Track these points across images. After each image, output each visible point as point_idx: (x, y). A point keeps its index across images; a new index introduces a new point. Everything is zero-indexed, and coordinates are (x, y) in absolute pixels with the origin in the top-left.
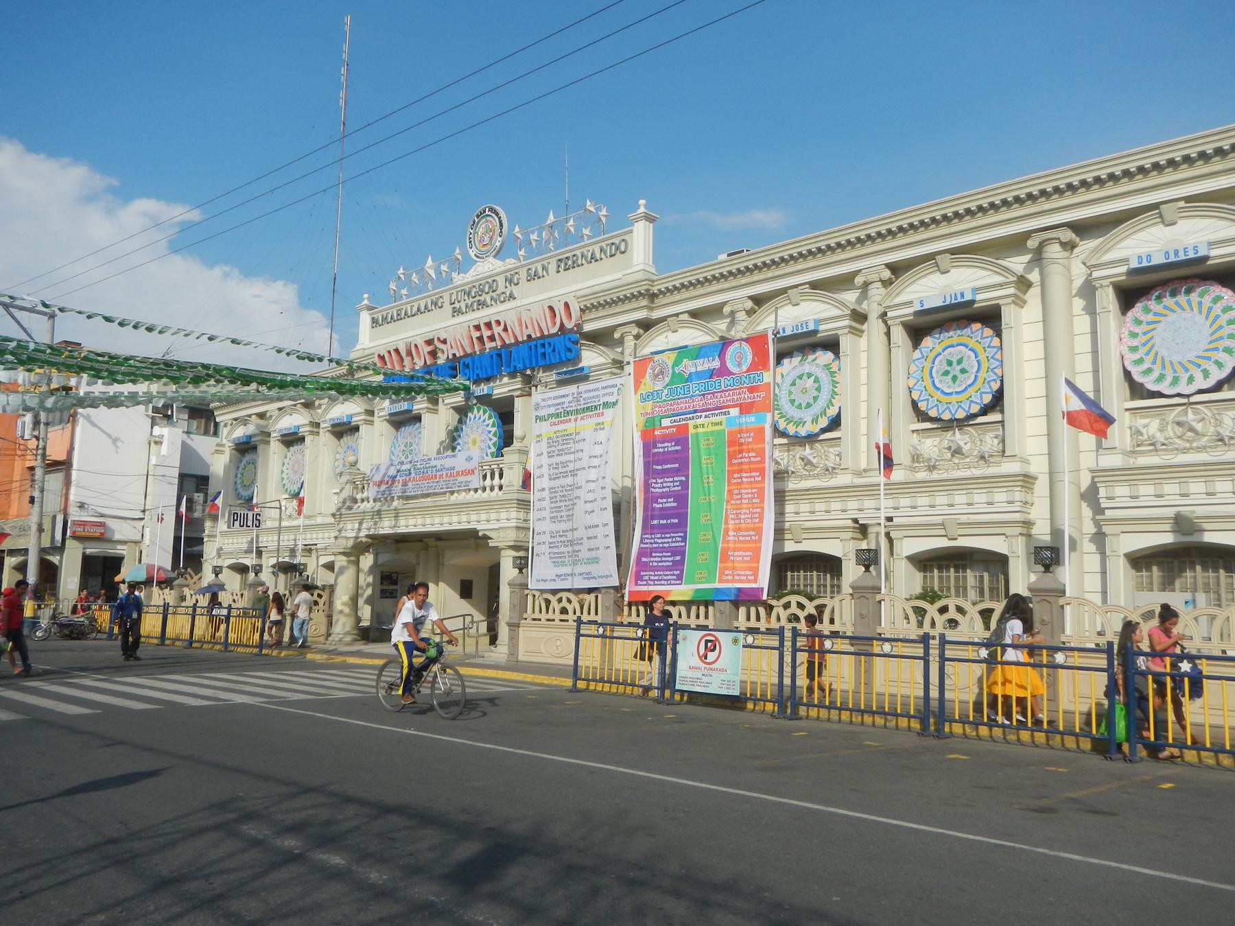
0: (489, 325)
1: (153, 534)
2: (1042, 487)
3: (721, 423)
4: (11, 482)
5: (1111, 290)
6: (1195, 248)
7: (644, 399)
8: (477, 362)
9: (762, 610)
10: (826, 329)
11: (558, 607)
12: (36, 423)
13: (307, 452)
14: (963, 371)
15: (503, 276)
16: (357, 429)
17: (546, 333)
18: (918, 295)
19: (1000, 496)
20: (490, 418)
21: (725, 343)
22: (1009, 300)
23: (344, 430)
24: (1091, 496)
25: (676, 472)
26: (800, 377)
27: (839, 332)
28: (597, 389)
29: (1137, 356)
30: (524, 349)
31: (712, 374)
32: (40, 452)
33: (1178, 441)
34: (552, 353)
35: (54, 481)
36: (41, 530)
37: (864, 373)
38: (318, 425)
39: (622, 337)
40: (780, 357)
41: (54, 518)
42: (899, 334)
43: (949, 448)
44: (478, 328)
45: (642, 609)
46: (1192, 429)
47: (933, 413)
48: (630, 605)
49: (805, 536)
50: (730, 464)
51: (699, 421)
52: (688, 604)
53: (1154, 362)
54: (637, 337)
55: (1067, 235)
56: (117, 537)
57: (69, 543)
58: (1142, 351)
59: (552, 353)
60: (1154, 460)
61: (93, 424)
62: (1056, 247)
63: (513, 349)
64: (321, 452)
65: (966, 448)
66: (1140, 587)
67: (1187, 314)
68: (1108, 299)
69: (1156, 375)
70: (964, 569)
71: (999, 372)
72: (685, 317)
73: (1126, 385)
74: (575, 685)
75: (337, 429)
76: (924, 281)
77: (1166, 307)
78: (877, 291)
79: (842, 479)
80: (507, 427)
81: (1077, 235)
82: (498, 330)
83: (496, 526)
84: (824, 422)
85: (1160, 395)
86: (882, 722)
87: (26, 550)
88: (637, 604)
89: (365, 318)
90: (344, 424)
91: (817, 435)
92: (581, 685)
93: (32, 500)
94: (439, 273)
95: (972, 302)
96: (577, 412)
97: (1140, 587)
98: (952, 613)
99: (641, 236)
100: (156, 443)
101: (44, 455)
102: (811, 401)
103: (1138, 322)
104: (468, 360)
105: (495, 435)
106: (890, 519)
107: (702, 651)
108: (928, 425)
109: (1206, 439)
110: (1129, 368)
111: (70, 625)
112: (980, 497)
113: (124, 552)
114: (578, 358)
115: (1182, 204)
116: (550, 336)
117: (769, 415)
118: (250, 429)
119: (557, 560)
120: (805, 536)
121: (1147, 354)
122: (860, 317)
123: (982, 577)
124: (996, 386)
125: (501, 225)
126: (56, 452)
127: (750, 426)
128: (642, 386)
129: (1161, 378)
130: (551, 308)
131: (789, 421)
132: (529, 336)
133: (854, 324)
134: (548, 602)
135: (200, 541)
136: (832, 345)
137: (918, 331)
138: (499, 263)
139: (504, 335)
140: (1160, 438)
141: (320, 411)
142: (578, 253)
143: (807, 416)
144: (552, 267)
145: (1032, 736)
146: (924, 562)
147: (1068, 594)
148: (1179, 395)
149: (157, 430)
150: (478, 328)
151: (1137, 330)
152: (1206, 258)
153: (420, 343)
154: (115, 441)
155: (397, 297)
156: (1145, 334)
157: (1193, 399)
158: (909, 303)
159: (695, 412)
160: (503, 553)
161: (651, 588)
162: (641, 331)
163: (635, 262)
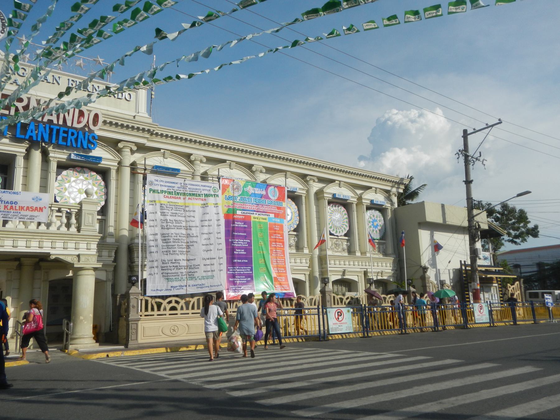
7: (228, 198)
9: (289, 302)
17: (69, 124)
25: (245, 237)
28: (198, 185)
31: (262, 196)
50: (270, 238)
51: (257, 216)
55: (317, 181)
83: (77, 253)
96: (184, 194)
107: (337, 316)
114: (90, 150)
128: (227, 192)
132: (50, 122)
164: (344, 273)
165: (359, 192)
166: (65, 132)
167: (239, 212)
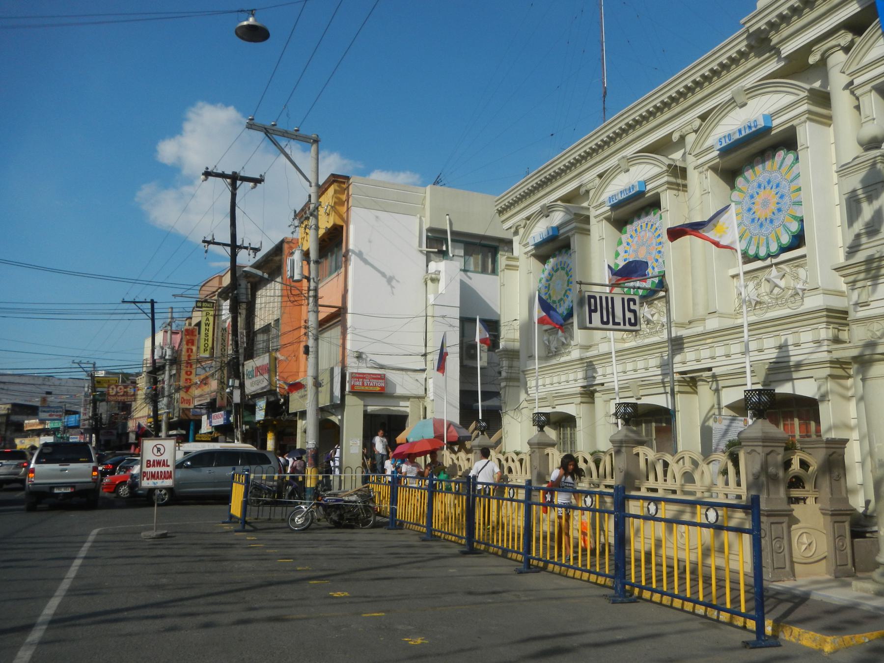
1: (436, 386)
32: (312, 293)
36: (317, 384)
38: (684, 171)
41: (332, 370)
56: (399, 391)
57: (350, 400)
61: (366, 262)
100: (433, 280)
111: (338, 507)
113: (408, 410)
118: (558, 217)
149: (433, 266)
154: (390, 280)
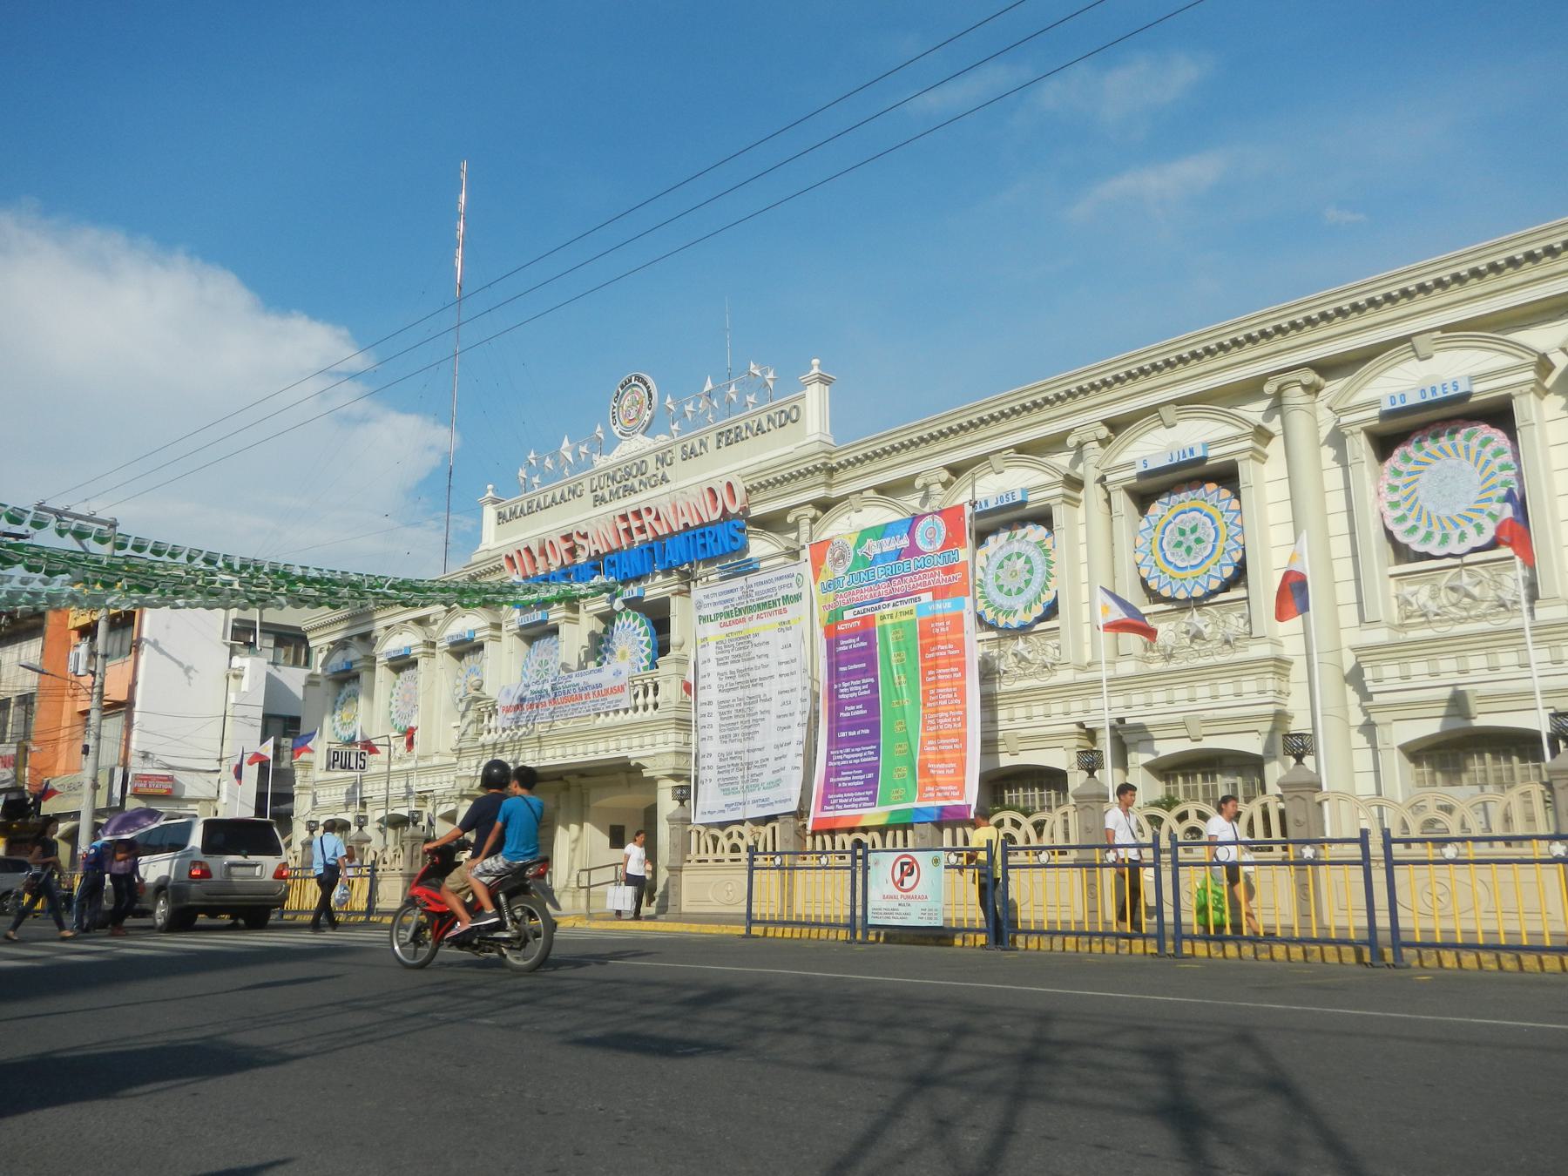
0: (637, 514)
2: (1298, 672)
3: (911, 612)
4: (59, 729)
5: (1363, 438)
6: (1455, 384)
8: (624, 559)
10: (1035, 500)
11: (727, 844)
12: (93, 654)
13: (421, 678)
14: (1198, 541)
15: (653, 457)
16: (480, 647)
18: (1139, 455)
19: (1249, 686)
20: (641, 625)
21: (916, 518)
22: (1247, 455)
23: (465, 649)
24: (1355, 678)
26: (1009, 558)
27: (1052, 502)
28: (770, 581)
29: (1399, 513)
30: (680, 543)
31: (899, 554)
33: (1453, 609)
34: (715, 543)
35: (113, 727)
37: (1083, 550)
38: (433, 645)
39: (797, 521)
40: (981, 537)
41: (112, 771)
42: (1122, 501)
43: (1187, 632)
44: (624, 518)
45: (827, 838)
46: (1468, 595)
47: (1166, 592)
48: (814, 834)
49: (1021, 747)
50: (924, 660)
51: (887, 611)
52: (882, 830)
53: (1419, 519)
54: (814, 520)
55: (1310, 377)
56: (188, 794)
58: (1405, 506)
59: (715, 543)
60: (1428, 633)
62: (1299, 389)
63: (667, 541)
64: (439, 679)
65: (1207, 632)
66: (1421, 784)
67: (1453, 461)
68: (1360, 447)
69: (1422, 533)
70: (1213, 774)
71: (1240, 539)
72: (871, 493)
73: (1389, 547)
74: (749, 930)
75: (457, 648)
76: (1147, 438)
77: (1428, 454)
78: (1093, 452)
79: (1064, 676)
80: (663, 637)
81: (1321, 375)
82: (648, 519)
84: (1038, 610)
85: (1428, 556)
86: (1113, 949)
87: (77, 815)
88: (822, 833)
89: (490, 513)
90: (464, 641)
91: (1031, 626)
92: (757, 930)
93: (86, 750)
94: (577, 455)
95: (1204, 459)
96: (749, 609)
97: (1421, 784)
98: (1193, 821)
99: (815, 400)
100: (235, 676)
101: (101, 694)
102: (1023, 585)
103: (1398, 473)
104: (613, 557)
105: (647, 645)
106: (1121, 721)
107: (898, 876)
108: (1162, 607)
109: (1485, 605)
110: (1390, 527)
112: (1226, 688)
114: (745, 549)
115: (1438, 334)
116: (711, 523)
117: (968, 601)
119: (726, 786)
120: (1021, 747)
121: (1410, 510)
122: (1075, 483)
123: (1235, 785)
124: (1237, 556)
125: (650, 396)
126: (115, 691)
127: (947, 613)
129: (1428, 537)
130: (711, 490)
131: (997, 611)
132: (686, 525)
133: (1068, 492)
134: (715, 839)
135: (290, 798)
136: (1044, 518)
137: (1143, 497)
138: (648, 440)
139: (655, 525)
140: (1432, 606)
141: (435, 628)
142: (742, 424)
143: (1019, 603)
144: (712, 443)
145: (1288, 952)
146: (1166, 770)
147: (1325, 788)
148: (1450, 555)
149: (237, 662)
150: (624, 518)
151: (1398, 482)
152: (1468, 395)
153: (556, 539)
155: (527, 486)
156: (1406, 486)
157: (1467, 559)
158: (1132, 464)
159: (882, 600)
160: (661, 784)
161: (838, 813)
162: (819, 513)
163: (809, 432)
164: (1458, 703)
165: (1543, 337)
166: (703, 535)
167: (848, 615)
